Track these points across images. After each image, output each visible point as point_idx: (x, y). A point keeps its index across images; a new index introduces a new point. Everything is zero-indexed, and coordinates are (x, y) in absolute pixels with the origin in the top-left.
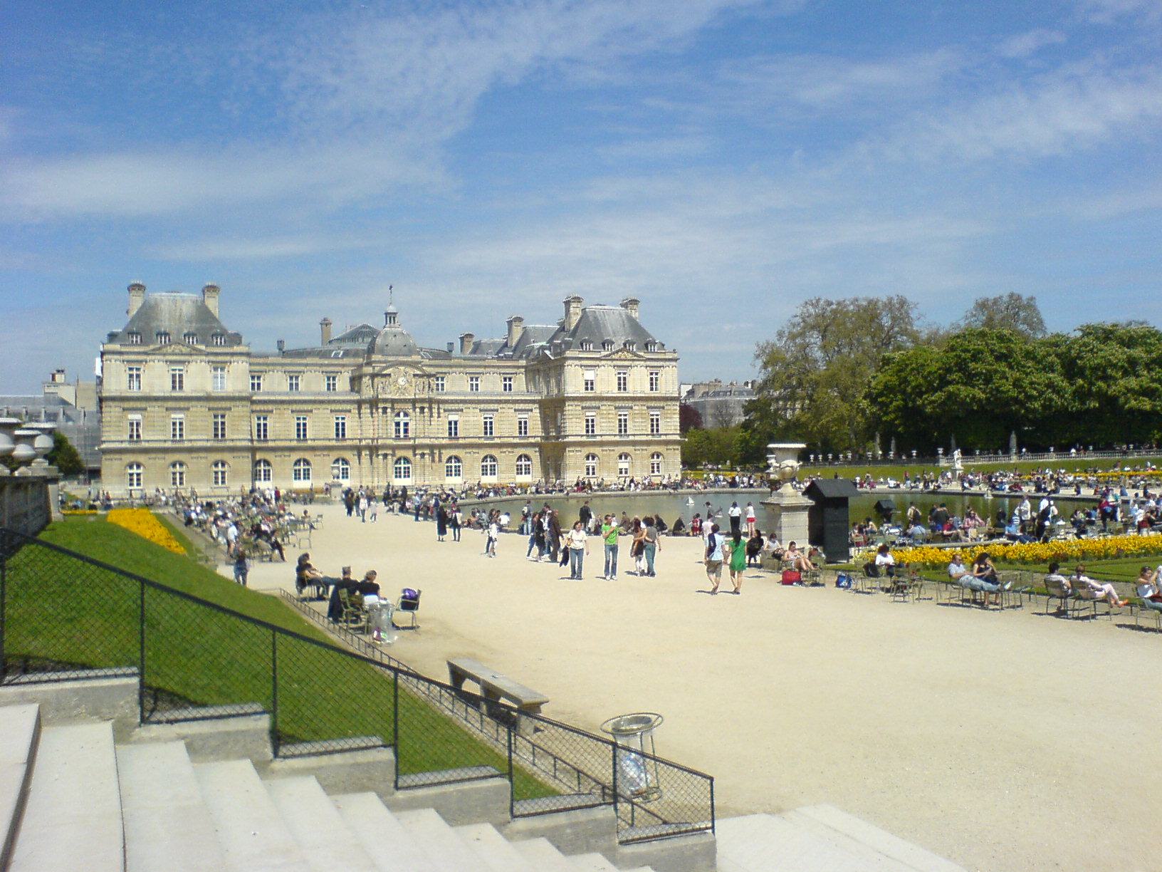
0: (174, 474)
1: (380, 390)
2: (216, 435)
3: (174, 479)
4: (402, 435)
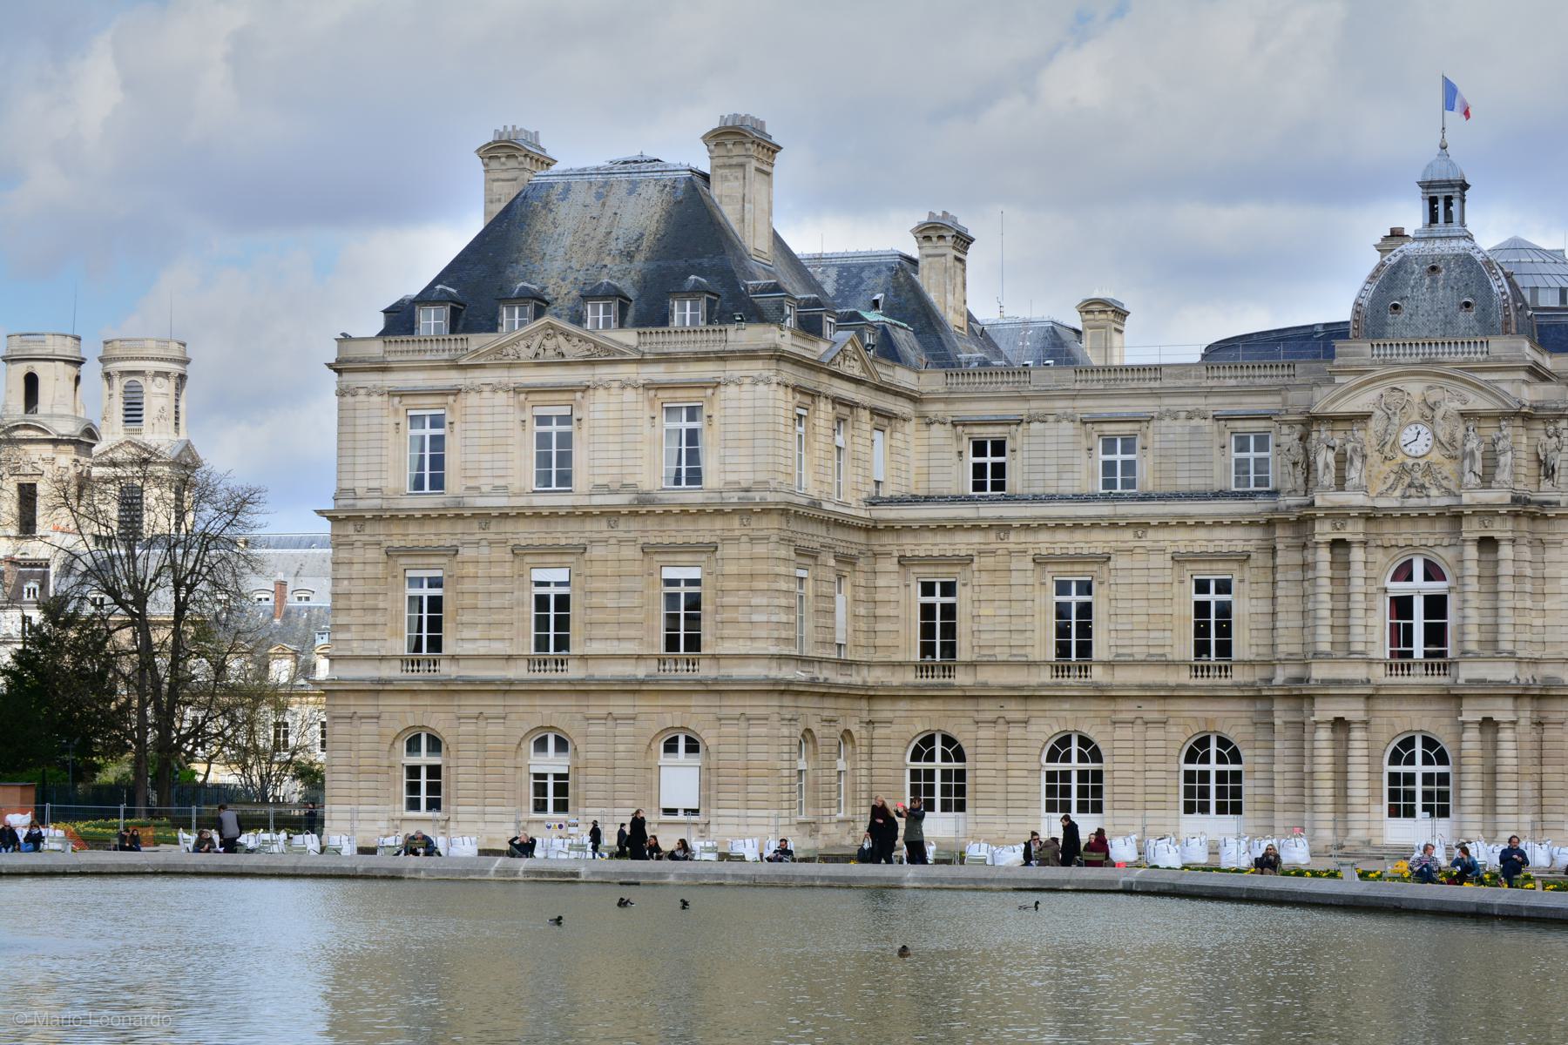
2: (672, 643)
4: (1418, 648)
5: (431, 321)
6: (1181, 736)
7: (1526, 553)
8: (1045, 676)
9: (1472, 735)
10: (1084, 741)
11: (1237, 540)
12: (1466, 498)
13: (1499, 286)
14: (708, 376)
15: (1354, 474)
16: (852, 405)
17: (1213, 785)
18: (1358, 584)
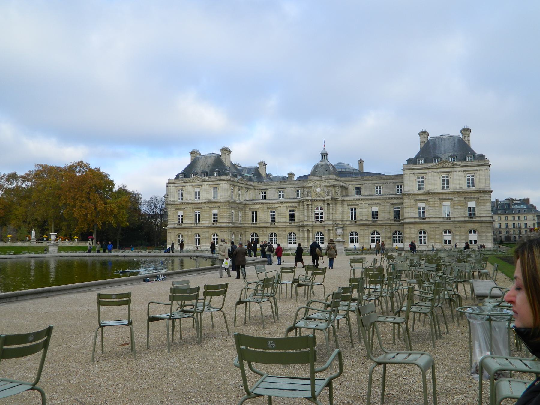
0: (196, 239)
1: (306, 196)
2: (214, 221)
3: (196, 242)
5: (181, 177)
6: (288, 232)
7: (334, 206)
8: (269, 225)
9: (326, 232)
10: (275, 234)
11: (295, 205)
12: (325, 198)
13: (331, 168)
15: (310, 195)
16: (242, 187)
18: (310, 210)
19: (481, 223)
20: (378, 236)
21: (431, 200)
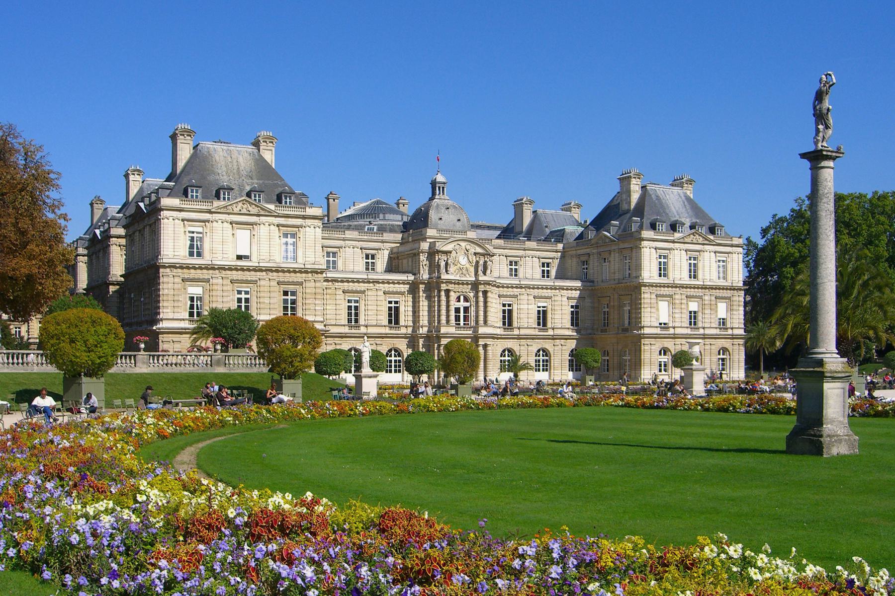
4: (462, 322)
9: (481, 348)
14: (299, 223)
15: (452, 269)
17: (393, 364)
19: (733, 338)
20: (545, 358)
21: (677, 297)
